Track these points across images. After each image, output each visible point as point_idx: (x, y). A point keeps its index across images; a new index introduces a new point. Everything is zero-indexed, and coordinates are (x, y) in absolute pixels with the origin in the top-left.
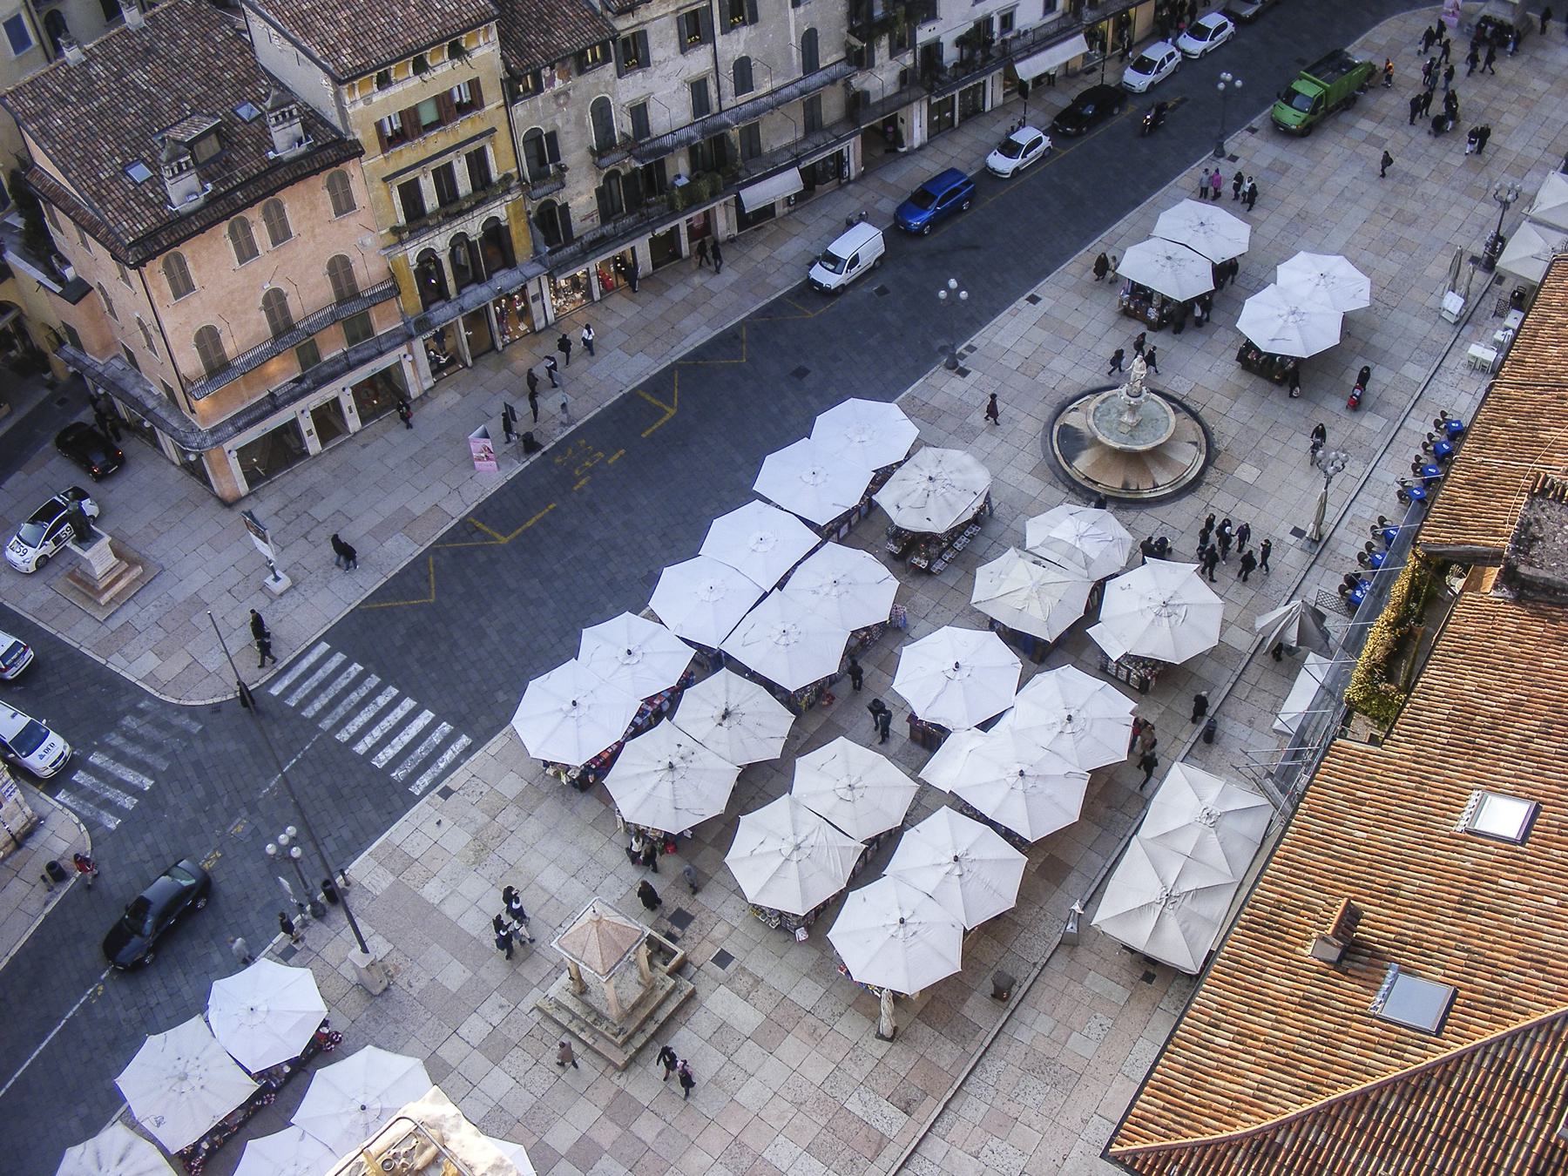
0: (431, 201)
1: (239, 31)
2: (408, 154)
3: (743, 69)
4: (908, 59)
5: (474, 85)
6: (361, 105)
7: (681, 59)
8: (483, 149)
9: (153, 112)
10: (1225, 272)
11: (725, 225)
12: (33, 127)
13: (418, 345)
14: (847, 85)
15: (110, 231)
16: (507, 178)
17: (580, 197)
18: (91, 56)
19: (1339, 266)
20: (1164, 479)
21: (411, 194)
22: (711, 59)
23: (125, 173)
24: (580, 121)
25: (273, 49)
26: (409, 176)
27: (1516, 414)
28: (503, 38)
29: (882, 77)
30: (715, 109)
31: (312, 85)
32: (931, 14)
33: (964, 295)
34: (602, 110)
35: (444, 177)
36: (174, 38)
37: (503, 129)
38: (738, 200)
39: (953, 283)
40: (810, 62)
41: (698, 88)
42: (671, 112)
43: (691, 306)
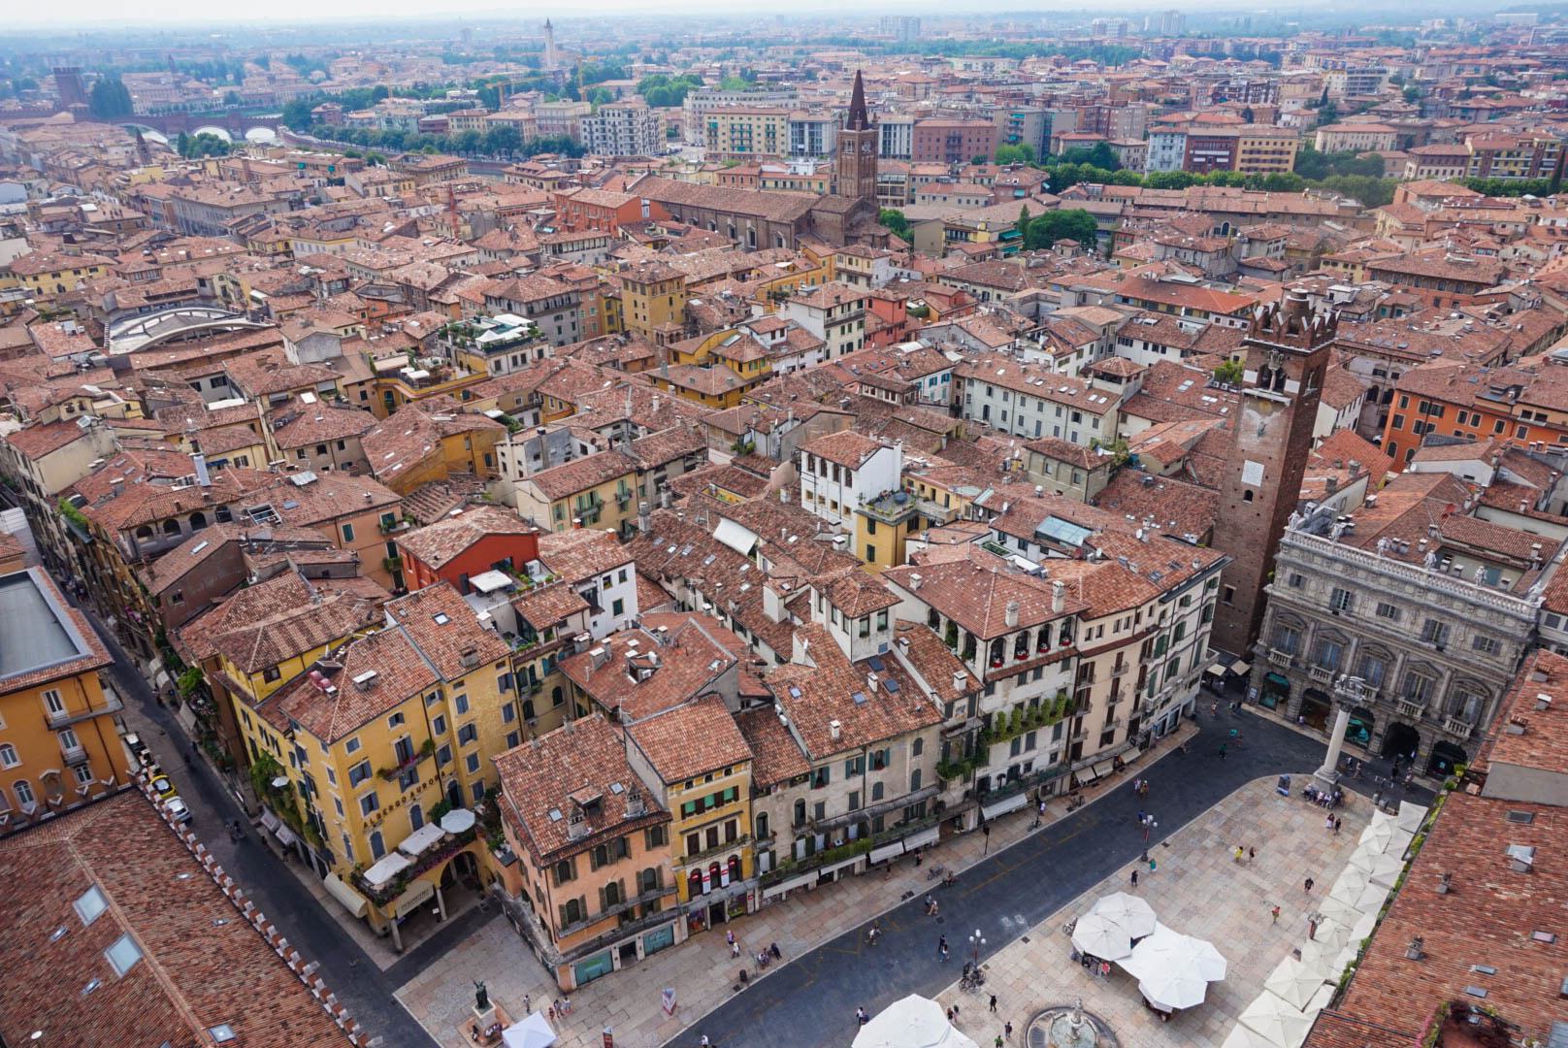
0: (703, 844)
2: (695, 821)
3: (878, 790)
5: (736, 789)
9: (568, 781)
13: (684, 919)
16: (744, 837)
21: (693, 842)
28: (754, 767)
29: (955, 792)
34: (801, 806)
35: (712, 834)
36: (587, 739)
37: (746, 811)
39: (978, 933)
40: (916, 784)
41: (853, 797)
43: (835, 914)
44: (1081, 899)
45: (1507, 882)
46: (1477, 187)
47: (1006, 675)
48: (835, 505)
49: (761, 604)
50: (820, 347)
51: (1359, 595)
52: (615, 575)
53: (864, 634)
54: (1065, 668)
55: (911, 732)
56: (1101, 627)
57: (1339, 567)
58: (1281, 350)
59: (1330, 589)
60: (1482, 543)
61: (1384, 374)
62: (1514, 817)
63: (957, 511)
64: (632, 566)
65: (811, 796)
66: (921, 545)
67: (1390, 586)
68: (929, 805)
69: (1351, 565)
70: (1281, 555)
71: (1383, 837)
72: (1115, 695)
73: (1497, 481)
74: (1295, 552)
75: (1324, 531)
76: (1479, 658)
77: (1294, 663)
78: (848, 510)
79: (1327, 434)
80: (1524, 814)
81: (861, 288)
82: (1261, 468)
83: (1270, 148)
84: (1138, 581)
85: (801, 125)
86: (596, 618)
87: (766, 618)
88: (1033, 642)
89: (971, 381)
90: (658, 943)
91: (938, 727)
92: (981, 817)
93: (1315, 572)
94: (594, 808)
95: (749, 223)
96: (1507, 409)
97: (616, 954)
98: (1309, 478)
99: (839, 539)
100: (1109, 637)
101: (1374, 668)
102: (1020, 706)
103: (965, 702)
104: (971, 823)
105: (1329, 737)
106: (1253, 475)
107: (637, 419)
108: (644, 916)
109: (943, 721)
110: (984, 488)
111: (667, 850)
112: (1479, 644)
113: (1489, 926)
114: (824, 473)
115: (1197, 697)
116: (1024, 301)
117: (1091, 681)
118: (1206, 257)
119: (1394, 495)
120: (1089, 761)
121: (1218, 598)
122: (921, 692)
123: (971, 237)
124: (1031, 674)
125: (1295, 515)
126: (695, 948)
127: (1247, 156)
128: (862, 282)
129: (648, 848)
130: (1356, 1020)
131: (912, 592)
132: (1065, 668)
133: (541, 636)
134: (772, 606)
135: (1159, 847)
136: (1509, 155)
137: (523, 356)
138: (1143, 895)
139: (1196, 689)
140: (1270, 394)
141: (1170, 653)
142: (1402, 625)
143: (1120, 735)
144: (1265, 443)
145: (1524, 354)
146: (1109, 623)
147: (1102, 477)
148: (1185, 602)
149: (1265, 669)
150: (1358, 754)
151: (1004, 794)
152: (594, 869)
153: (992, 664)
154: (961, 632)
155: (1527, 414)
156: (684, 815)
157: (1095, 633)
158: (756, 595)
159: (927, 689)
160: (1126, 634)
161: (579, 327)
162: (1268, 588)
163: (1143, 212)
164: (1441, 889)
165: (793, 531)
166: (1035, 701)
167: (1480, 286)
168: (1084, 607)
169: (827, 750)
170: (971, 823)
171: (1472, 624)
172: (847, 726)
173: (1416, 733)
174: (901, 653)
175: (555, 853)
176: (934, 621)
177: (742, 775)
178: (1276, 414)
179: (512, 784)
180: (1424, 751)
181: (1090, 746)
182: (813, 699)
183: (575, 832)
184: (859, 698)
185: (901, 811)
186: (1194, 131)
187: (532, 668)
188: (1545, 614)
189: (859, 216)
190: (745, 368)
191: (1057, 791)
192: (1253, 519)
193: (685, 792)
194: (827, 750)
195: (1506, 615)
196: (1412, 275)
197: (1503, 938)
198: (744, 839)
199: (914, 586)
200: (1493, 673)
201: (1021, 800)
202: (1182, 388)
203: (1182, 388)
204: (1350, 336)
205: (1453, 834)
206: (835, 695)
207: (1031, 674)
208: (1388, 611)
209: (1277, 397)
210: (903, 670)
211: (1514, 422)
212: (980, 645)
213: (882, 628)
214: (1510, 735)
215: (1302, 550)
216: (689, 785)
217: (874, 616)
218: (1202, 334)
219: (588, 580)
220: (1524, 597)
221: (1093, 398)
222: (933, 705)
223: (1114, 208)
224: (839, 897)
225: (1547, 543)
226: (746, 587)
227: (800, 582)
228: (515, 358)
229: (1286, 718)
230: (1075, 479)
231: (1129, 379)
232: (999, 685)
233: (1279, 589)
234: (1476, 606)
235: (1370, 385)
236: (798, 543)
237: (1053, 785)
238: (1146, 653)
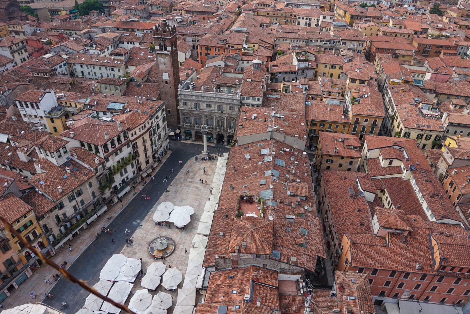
3: (82, 202)
5: (31, 221)
8: (35, 231)
13: (28, 269)
20: (168, 252)
24: (53, 220)
27: (213, 240)
28: (35, 212)
29: (107, 193)
34: (57, 217)
37: (38, 226)
39: (127, 230)
41: (75, 207)
43: (82, 243)
44: (153, 208)
45: (246, 164)
47: (111, 154)
48: (36, 117)
49: (18, 157)
50: (12, 61)
51: (200, 103)
53: (60, 156)
54: (128, 146)
55: (86, 181)
56: (135, 132)
57: (194, 97)
58: (163, 38)
59: (193, 104)
60: (226, 82)
61: (195, 41)
62: (245, 148)
63: (81, 108)
65: (60, 213)
66: (71, 122)
68: (101, 200)
70: (179, 98)
71: (221, 163)
72: (146, 150)
73: (226, 65)
74: (182, 96)
75: (188, 88)
76: (231, 112)
77: (190, 126)
78: (41, 117)
79: (184, 61)
80: (246, 147)
81: (22, 37)
82: (167, 74)
84: (142, 115)
87: (22, 162)
88: (116, 142)
89: (74, 64)
90: (22, 280)
91: (95, 176)
92: (118, 197)
93: (189, 100)
97: (6, 291)
98: (181, 74)
99: (40, 128)
100: (138, 134)
101: (209, 122)
102: (119, 162)
103: (101, 166)
104: (116, 200)
106: (166, 76)
108: (12, 275)
109: (95, 174)
110: (87, 98)
111: (12, 250)
112: (231, 108)
113: (244, 176)
114: (27, 107)
115: (169, 143)
116: (84, 34)
117: (137, 148)
118: (139, 12)
119: (203, 74)
120: (144, 170)
121: (166, 114)
122: (86, 168)
124: (119, 151)
125: (179, 85)
126: (37, 275)
128: (22, 34)
129: (4, 253)
130: (223, 209)
131: (72, 138)
132: (128, 146)
134: (23, 157)
135: (170, 186)
138: (169, 201)
139: (168, 141)
140: (164, 52)
141: (157, 133)
143: (151, 160)
145: (227, 30)
146: (137, 130)
147: (124, 87)
148: (157, 118)
149: (184, 130)
151: (122, 188)
153: (105, 152)
154: (92, 146)
155: (229, 46)
157: (134, 134)
158: (15, 155)
159: (87, 166)
160: (143, 131)
162: (178, 108)
164: (233, 171)
166: (123, 159)
167: (213, 13)
168: (128, 127)
169: (59, 197)
170: (116, 200)
172: (64, 187)
174: (75, 158)
176: (83, 145)
177: (31, 216)
178: (167, 58)
181: (143, 166)
182: (48, 183)
184: (65, 177)
185: (92, 205)
191: (138, 182)
192: (169, 89)
196: (196, 11)
197: (248, 177)
198: (41, 235)
199: (72, 136)
201: (128, 188)
202: (142, 54)
203: (142, 54)
204: (184, 31)
205: (234, 157)
206: (56, 179)
207: (119, 151)
208: (208, 106)
209: (166, 52)
211: (227, 49)
212: (100, 148)
213: (65, 152)
215: (184, 95)
217: (61, 150)
218: (143, 37)
220: (237, 94)
221: (116, 62)
222: (91, 170)
224: (81, 238)
226: (10, 154)
227: (30, 146)
229: (193, 141)
230: (116, 89)
231: (125, 55)
232: (110, 158)
233: (181, 107)
234: (227, 99)
235: (192, 45)
237: (136, 180)
238: (150, 135)
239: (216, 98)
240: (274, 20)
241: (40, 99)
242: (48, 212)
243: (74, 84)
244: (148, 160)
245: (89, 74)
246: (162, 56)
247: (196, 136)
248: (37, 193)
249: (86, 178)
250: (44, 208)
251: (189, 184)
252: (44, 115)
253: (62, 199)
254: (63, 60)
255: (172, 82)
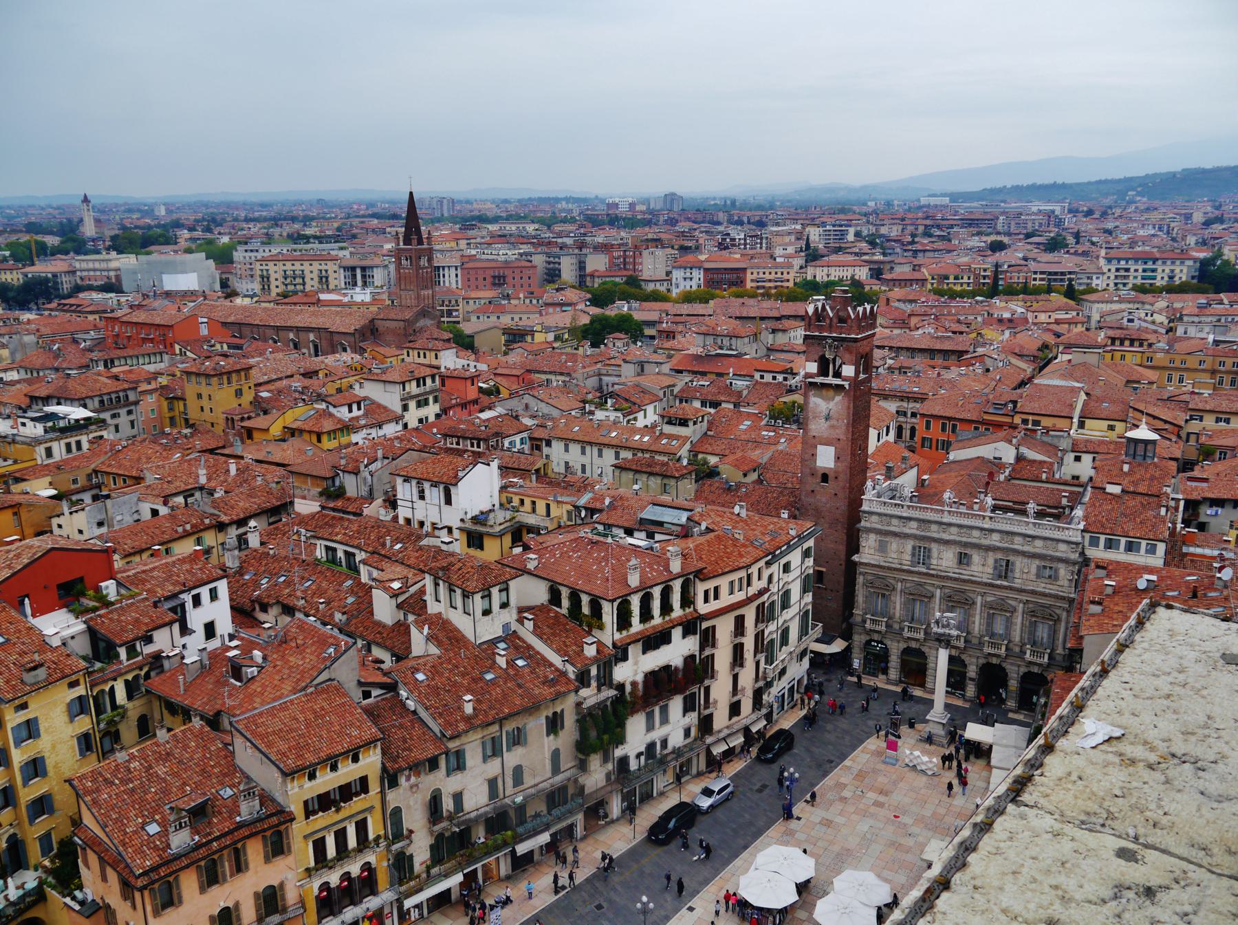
0: (331, 851)
1: (226, 745)
2: (322, 819)
3: (518, 772)
4: (610, 766)
5: (364, 781)
6: (297, 790)
7: (484, 766)
8: (365, 819)
9: (166, 792)
10: (802, 888)
11: (504, 868)
12: (88, 799)
14: (576, 781)
15: (127, 866)
16: (378, 837)
17: (420, 850)
18: (132, 757)
19: (870, 877)
21: (320, 846)
22: (500, 766)
23: (143, 828)
25: (246, 757)
26: (319, 835)
28: (384, 753)
29: (596, 775)
30: (501, 796)
31: (266, 776)
32: (621, 740)
33: (651, 905)
35: (341, 836)
36: (185, 747)
37: (378, 806)
38: (513, 852)
40: (556, 770)
41: (492, 783)
42: (476, 800)
44: (738, 862)
46: (939, 293)
50: (397, 419)
52: (204, 592)
53: (487, 612)
56: (716, 589)
59: (909, 548)
61: (905, 414)
63: (560, 518)
64: (224, 581)
65: (447, 784)
67: (959, 534)
68: (571, 791)
69: (923, 521)
70: (863, 523)
73: (1020, 458)
83: (772, 276)
84: (744, 546)
85: (353, 269)
86: (186, 640)
87: (379, 624)
93: (895, 534)
94: (199, 814)
95: (312, 336)
96: (1008, 420)
100: (726, 600)
105: (932, 692)
106: (826, 458)
107: (213, 484)
117: (714, 646)
120: (722, 735)
122: (551, 665)
123: (529, 338)
127: (754, 284)
133: (123, 652)
134: (384, 610)
136: (956, 278)
137: (79, 443)
142: (974, 568)
143: (747, 705)
144: (832, 427)
146: (723, 583)
149: (864, 638)
150: (959, 703)
152: (203, 890)
153: (620, 629)
154: (585, 599)
155: (1025, 422)
156: (308, 813)
159: (556, 659)
160: (740, 596)
161: (139, 425)
162: (856, 558)
163: (678, 319)
165: (397, 541)
171: (1034, 556)
172: (478, 701)
173: (1004, 669)
174: (527, 632)
175: (154, 869)
176: (555, 598)
177: (371, 762)
178: (838, 398)
179: (95, 802)
180: (1013, 684)
181: (721, 719)
183: (180, 839)
184: (489, 677)
186: (708, 265)
187: (112, 688)
188: (1087, 536)
189: (421, 323)
190: (325, 438)
191: (694, 771)
192: (828, 499)
193: (308, 785)
194: (462, 726)
195: (1058, 541)
196: (908, 349)
200: (1056, 597)
206: (463, 675)
208: (963, 559)
209: (838, 381)
210: (529, 647)
213: (504, 605)
214: (1093, 615)
215: (879, 514)
216: (312, 776)
217: (495, 591)
219: (175, 596)
222: (564, 674)
223: (653, 316)
225: (1071, 493)
226: (350, 600)
228: (68, 446)
229: (889, 682)
231: (695, 423)
232: (630, 649)
236: (404, 549)
237: (689, 761)
239: (992, 531)
240: (1170, 380)
241: (461, 474)
242: (415, 768)
243: (546, 474)
244: (739, 702)
245: (584, 471)
246: (824, 392)
247: (904, 665)
248: (403, 705)
249: (547, 691)
250: (410, 750)
251: (873, 809)
252: (459, 524)
253: (464, 739)
254: (522, 428)
255: (842, 477)
